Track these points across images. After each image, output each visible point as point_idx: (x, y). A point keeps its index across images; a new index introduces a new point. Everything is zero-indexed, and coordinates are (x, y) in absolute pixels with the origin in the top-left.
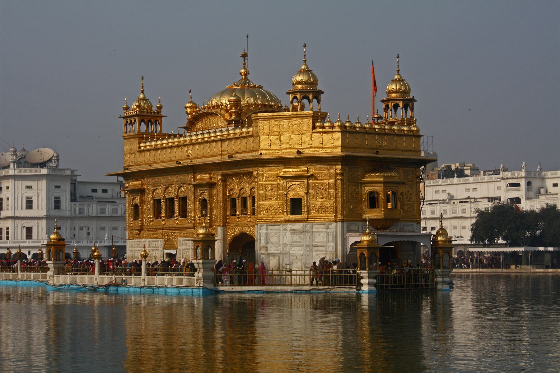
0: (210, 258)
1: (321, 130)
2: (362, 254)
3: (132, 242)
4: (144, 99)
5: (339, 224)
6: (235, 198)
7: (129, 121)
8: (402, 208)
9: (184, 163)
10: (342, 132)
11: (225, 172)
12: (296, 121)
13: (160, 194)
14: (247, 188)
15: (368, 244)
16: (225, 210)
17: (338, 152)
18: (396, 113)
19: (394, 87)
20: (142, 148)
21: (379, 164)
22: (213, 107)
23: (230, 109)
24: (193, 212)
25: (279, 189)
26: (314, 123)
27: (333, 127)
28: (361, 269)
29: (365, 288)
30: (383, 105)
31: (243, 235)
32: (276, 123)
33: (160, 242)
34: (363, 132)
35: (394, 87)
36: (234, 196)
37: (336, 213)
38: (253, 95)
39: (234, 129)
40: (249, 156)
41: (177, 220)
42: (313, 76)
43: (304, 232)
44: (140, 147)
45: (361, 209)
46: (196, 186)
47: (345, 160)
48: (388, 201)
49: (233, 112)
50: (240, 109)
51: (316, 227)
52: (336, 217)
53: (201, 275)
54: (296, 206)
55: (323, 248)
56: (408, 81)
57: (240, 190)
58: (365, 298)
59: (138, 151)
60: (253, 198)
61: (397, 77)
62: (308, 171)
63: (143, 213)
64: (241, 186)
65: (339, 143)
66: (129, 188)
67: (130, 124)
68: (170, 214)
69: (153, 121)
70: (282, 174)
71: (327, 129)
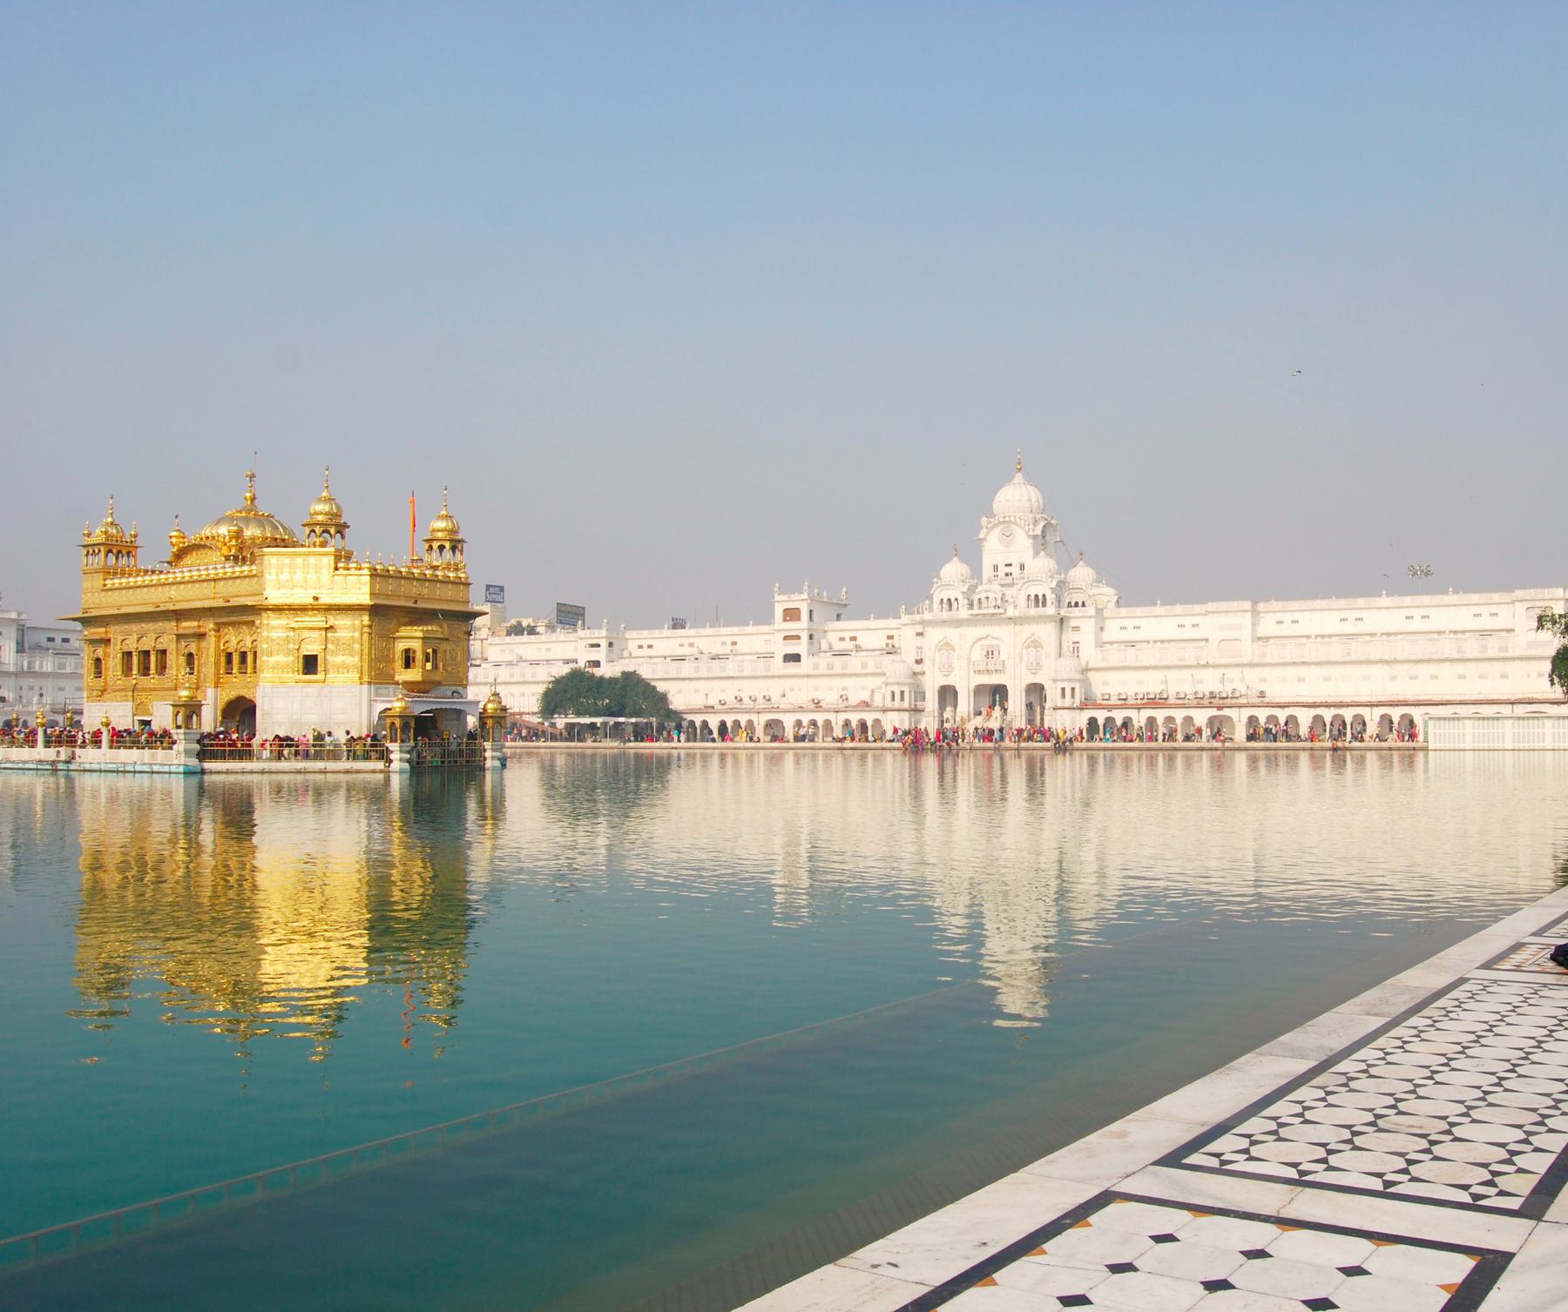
5: (365, 687)
13: (131, 645)
14: (248, 640)
17: (366, 600)
19: (442, 524)
21: (418, 616)
29: (396, 766)
30: (426, 546)
34: (399, 576)
35: (442, 524)
38: (262, 526)
40: (249, 602)
46: (179, 637)
47: (375, 611)
48: (428, 660)
54: (310, 664)
61: (444, 512)
65: (367, 589)
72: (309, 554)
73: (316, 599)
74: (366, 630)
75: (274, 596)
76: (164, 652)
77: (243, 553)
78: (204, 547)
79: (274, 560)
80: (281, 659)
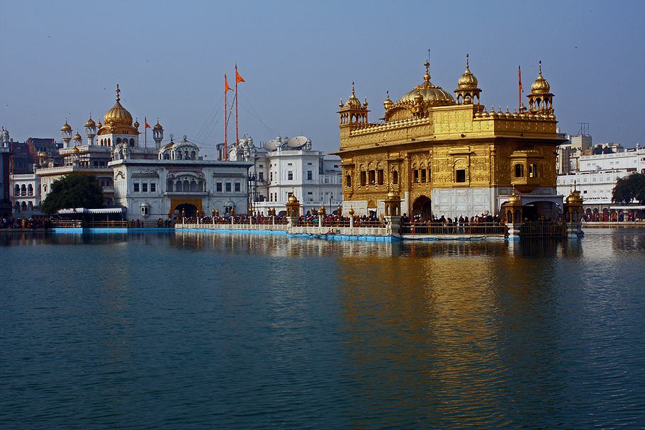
1: (479, 119)
2: (509, 211)
5: (493, 189)
8: (542, 176)
9: (381, 145)
11: (410, 151)
12: (461, 112)
13: (365, 168)
14: (426, 162)
17: (492, 135)
19: (538, 85)
21: (522, 144)
22: (404, 103)
25: (448, 163)
26: (474, 114)
27: (489, 116)
29: (511, 236)
30: (529, 100)
31: (423, 198)
32: (446, 114)
33: (365, 203)
34: (511, 119)
35: (538, 85)
42: (474, 78)
44: (351, 134)
45: (510, 177)
46: (390, 162)
51: (476, 191)
52: (490, 183)
53: (390, 227)
54: (460, 176)
56: (548, 81)
58: (511, 244)
61: (539, 78)
62: (469, 150)
63: (353, 182)
64: (421, 161)
65: (492, 128)
66: (344, 164)
70: (450, 152)
71: (484, 118)
73: (463, 136)
75: (440, 136)
76: (382, 171)
77: (423, 110)
78: (403, 108)
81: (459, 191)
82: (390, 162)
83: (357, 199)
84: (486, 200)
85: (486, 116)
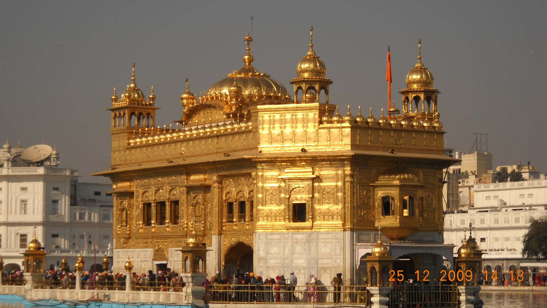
0: (201, 271)
2: (373, 268)
3: (119, 252)
4: (135, 90)
5: (348, 234)
6: (232, 203)
7: (118, 115)
8: (421, 214)
10: (352, 128)
13: (151, 197)
14: (246, 190)
15: (379, 257)
16: (221, 217)
18: (417, 106)
19: (416, 77)
20: (132, 144)
21: (394, 166)
23: (230, 101)
24: (185, 217)
25: (280, 192)
26: (321, 116)
27: (342, 122)
28: (372, 285)
30: (403, 98)
33: (150, 252)
34: (377, 128)
36: (230, 200)
37: (345, 221)
39: (232, 124)
41: (168, 227)
42: (322, 65)
43: (309, 241)
44: (129, 144)
47: (356, 161)
49: (233, 105)
50: (241, 100)
52: (344, 225)
53: (189, 290)
54: (299, 213)
55: (329, 261)
57: (238, 194)
59: (127, 149)
60: (252, 202)
62: (313, 173)
64: (239, 188)
65: (348, 141)
67: (119, 117)
68: (161, 220)
69: (144, 113)
72: (297, 109)
73: (303, 150)
74: (348, 179)
75: (267, 148)
77: (243, 111)
79: (266, 117)
80: (275, 208)
81: (296, 236)
82: (190, 189)
83: (135, 247)
84: (338, 251)
85: (339, 122)
